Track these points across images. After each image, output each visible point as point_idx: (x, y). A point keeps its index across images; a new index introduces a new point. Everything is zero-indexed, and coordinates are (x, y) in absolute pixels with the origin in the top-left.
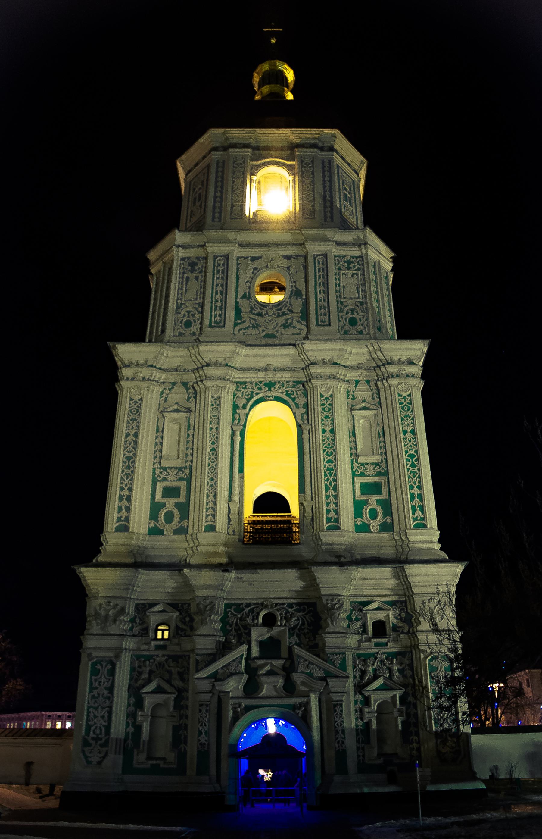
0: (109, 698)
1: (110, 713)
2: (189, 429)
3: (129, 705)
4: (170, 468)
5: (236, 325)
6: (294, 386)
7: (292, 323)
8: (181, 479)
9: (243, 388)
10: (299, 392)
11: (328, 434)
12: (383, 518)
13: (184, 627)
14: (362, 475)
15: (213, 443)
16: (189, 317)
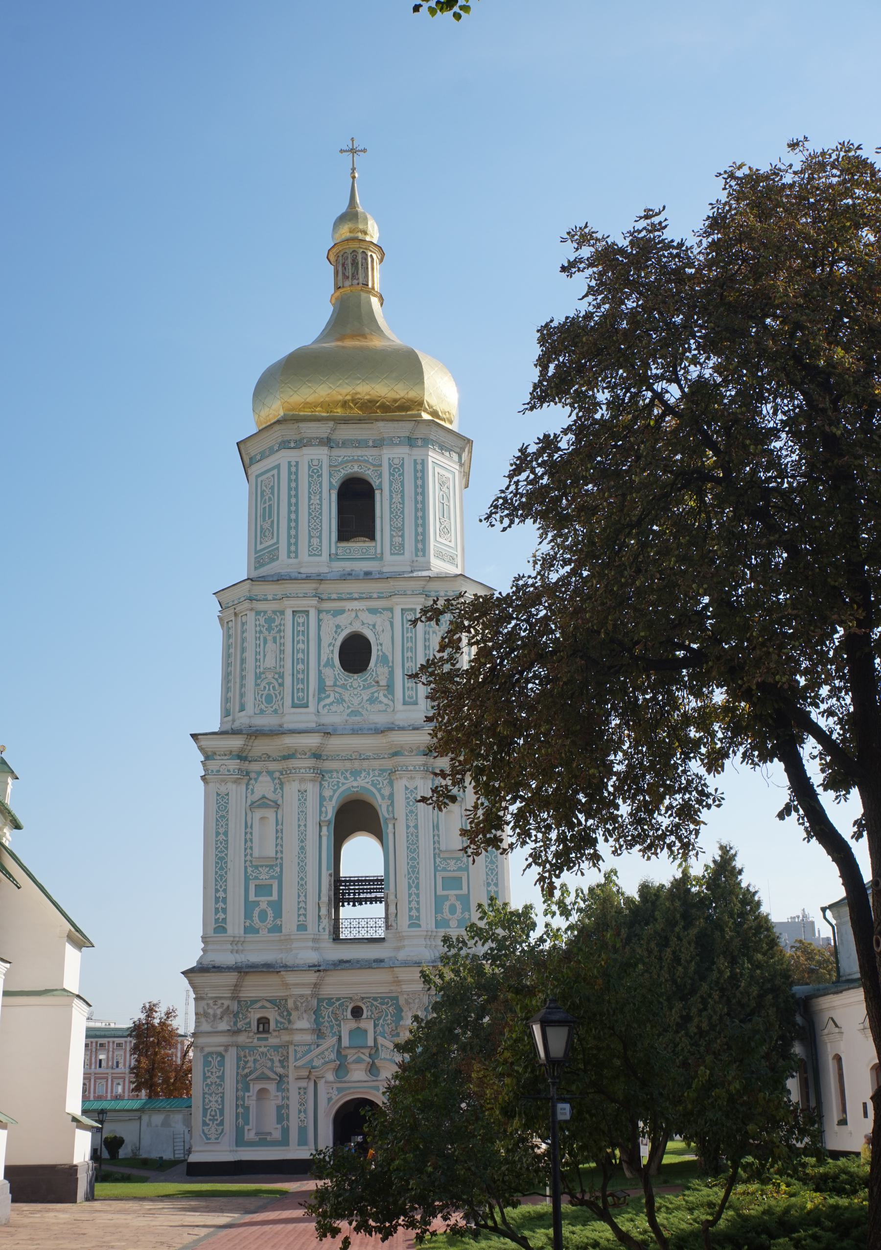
0: (221, 1085)
1: (222, 1098)
2: (277, 824)
3: (237, 1090)
4: (262, 866)
5: (320, 700)
6: (379, 776)
7: (377, 698)
8: (272, 877)
9: (331, 778)
10: (385, 782)
11: (412, 830)
12: (462, 913)
13: (282, 1020)
14: (444, 870)
15: (302, 841)
16: (269, 690)
